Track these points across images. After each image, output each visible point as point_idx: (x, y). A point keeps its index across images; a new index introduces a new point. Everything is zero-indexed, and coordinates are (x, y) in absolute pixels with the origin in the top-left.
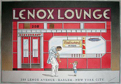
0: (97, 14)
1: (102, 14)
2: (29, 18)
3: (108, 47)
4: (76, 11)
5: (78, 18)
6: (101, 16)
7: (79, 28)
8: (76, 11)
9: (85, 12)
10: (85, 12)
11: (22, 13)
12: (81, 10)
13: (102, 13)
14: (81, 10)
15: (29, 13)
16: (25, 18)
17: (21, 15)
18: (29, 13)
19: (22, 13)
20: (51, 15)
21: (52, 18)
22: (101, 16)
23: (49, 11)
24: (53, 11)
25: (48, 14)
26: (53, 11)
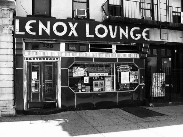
0: (135, 32)
1: (141, 34)
2: (40, 33)
3: (159, 98)
4: (110, 27)
5: (113, 37)
6: (139, 36)
7: (111, 51)
8: (110, 27)
9: (121, 30)
10: (121, 30)
11: (31, 25)
12: (116, 27)
13: (140, 32)
14: (116, 27)
15: (41, 26)
16: (34, 34)
17: (28, 27)
18: (41, 26)
19: (31, 25)
20: (74, 32)
21: (76, 35)
22: (139, 36)
23: (71, 24)
24: (76, 24)
25: (69, 29)
26: (76, 24)
